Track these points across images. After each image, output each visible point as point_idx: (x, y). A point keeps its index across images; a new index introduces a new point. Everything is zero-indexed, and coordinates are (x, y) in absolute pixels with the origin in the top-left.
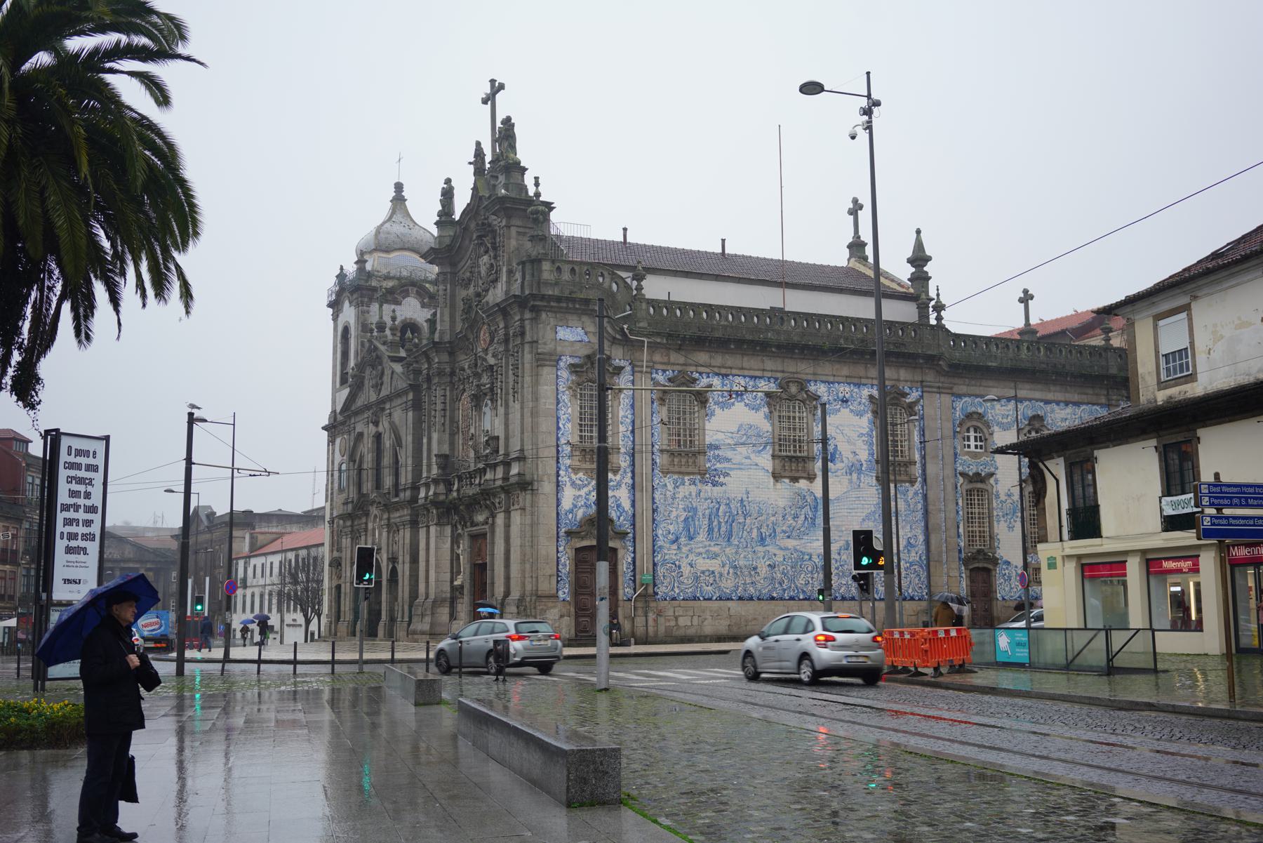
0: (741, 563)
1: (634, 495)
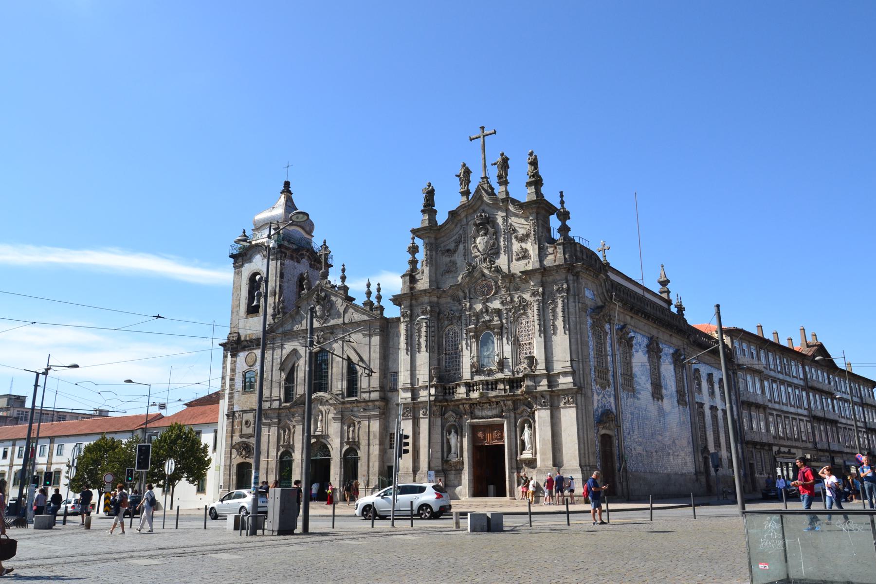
1: (616, 402)
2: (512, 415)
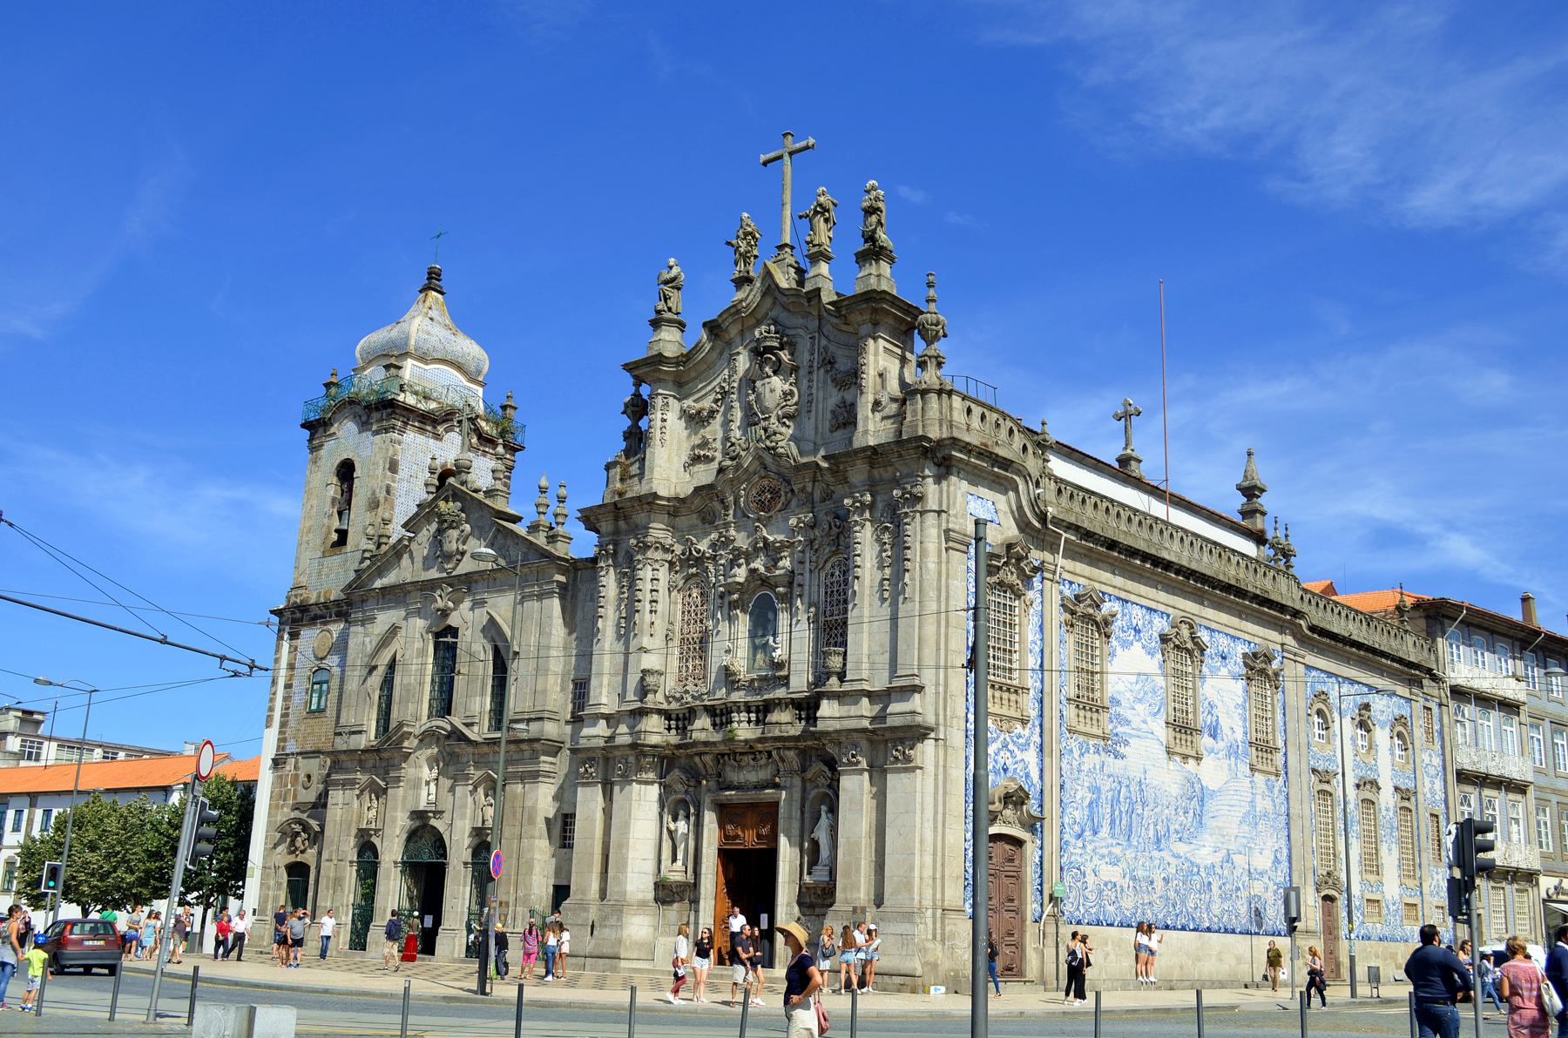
0: (1140, 872)
2: (797, 781)
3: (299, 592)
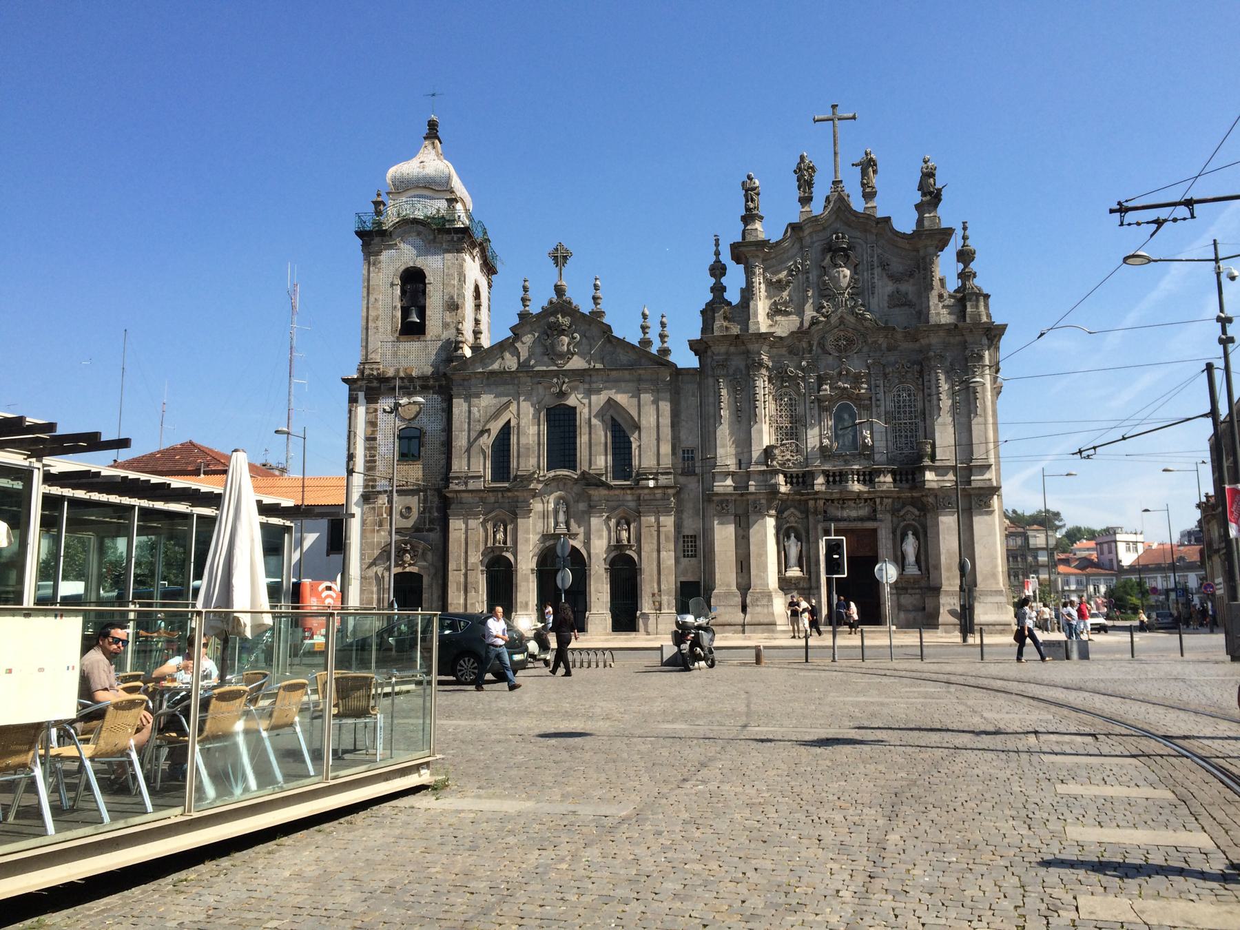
3: (375, 366)
